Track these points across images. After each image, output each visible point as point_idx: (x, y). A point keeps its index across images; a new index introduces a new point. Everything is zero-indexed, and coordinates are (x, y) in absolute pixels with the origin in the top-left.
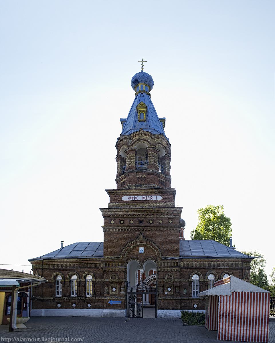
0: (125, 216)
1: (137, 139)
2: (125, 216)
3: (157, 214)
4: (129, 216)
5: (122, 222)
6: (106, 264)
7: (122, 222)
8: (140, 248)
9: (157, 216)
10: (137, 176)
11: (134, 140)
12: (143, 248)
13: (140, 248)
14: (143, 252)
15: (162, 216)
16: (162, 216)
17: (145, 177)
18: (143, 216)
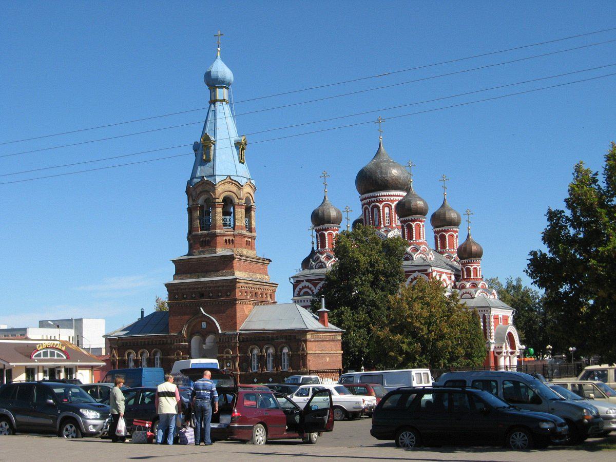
0: (187, 290)
1: (201, 190)
2: (187, 290)
3: (217, 287)
4: (191, 290)
5: (185, 296)
6: (171, 341)
7: (185, 296)
8: (203, 323)
9: (216, 288)
10: (201, 240)
11: (198, 192)
12: (205, 323)
13: (203, 323)
14: (205, 327)
15: (220, 288)
16: (220, 288)
17: (208, 240)
18: (203, 289)
